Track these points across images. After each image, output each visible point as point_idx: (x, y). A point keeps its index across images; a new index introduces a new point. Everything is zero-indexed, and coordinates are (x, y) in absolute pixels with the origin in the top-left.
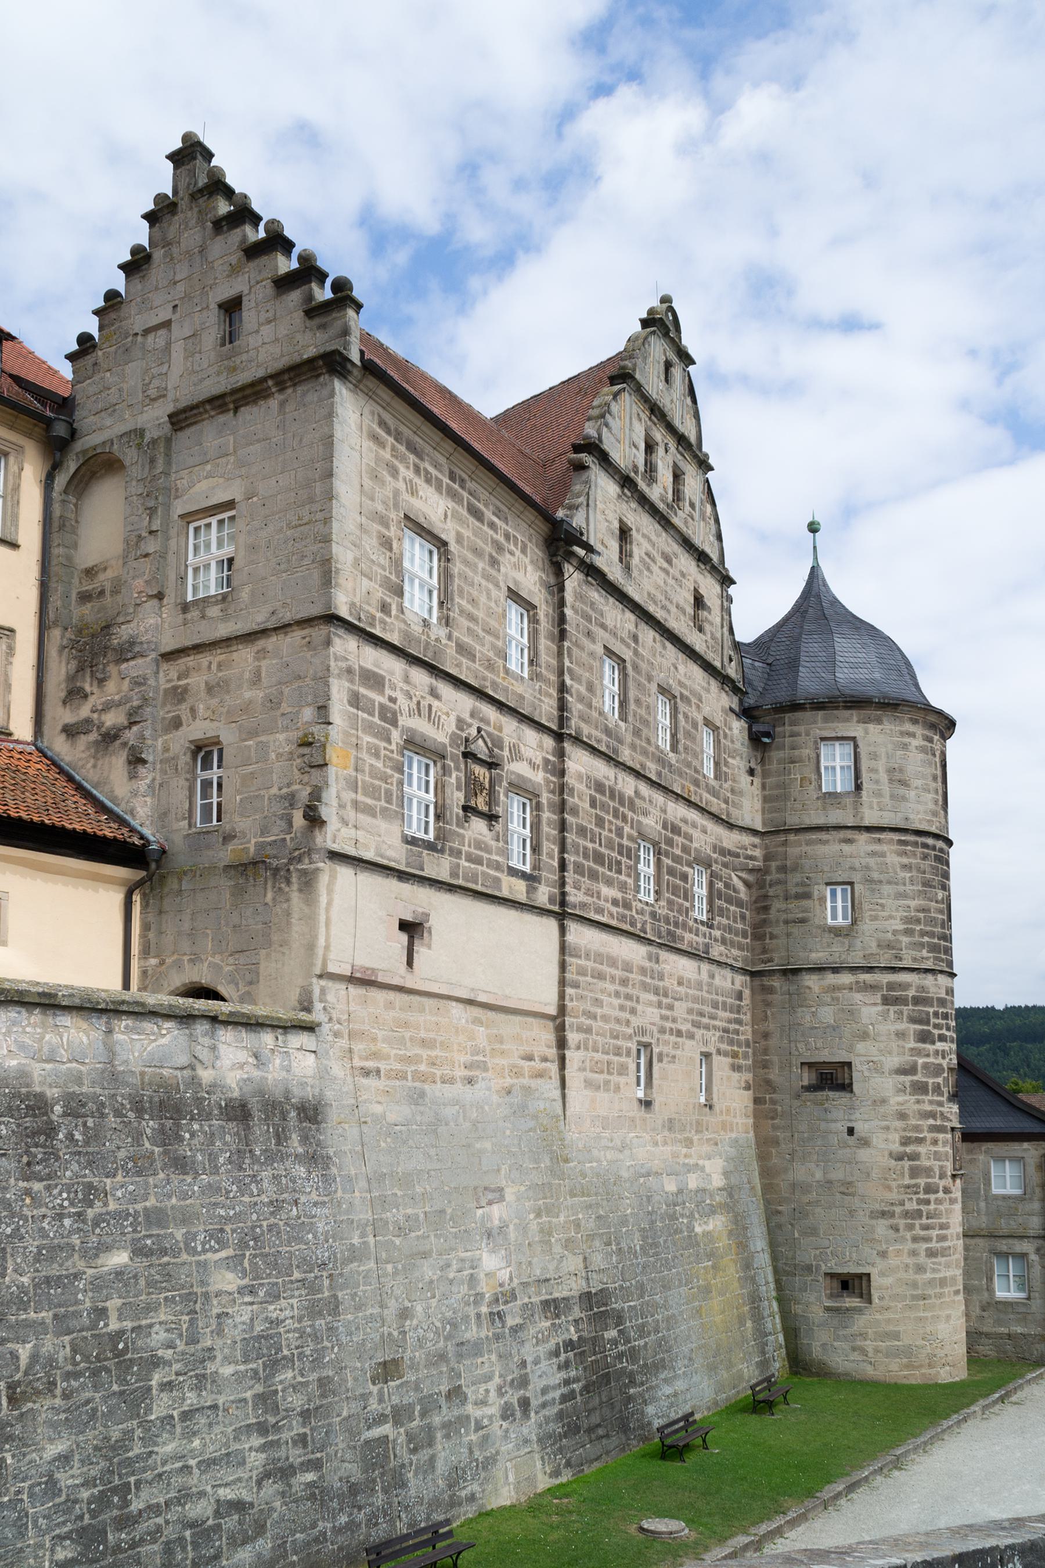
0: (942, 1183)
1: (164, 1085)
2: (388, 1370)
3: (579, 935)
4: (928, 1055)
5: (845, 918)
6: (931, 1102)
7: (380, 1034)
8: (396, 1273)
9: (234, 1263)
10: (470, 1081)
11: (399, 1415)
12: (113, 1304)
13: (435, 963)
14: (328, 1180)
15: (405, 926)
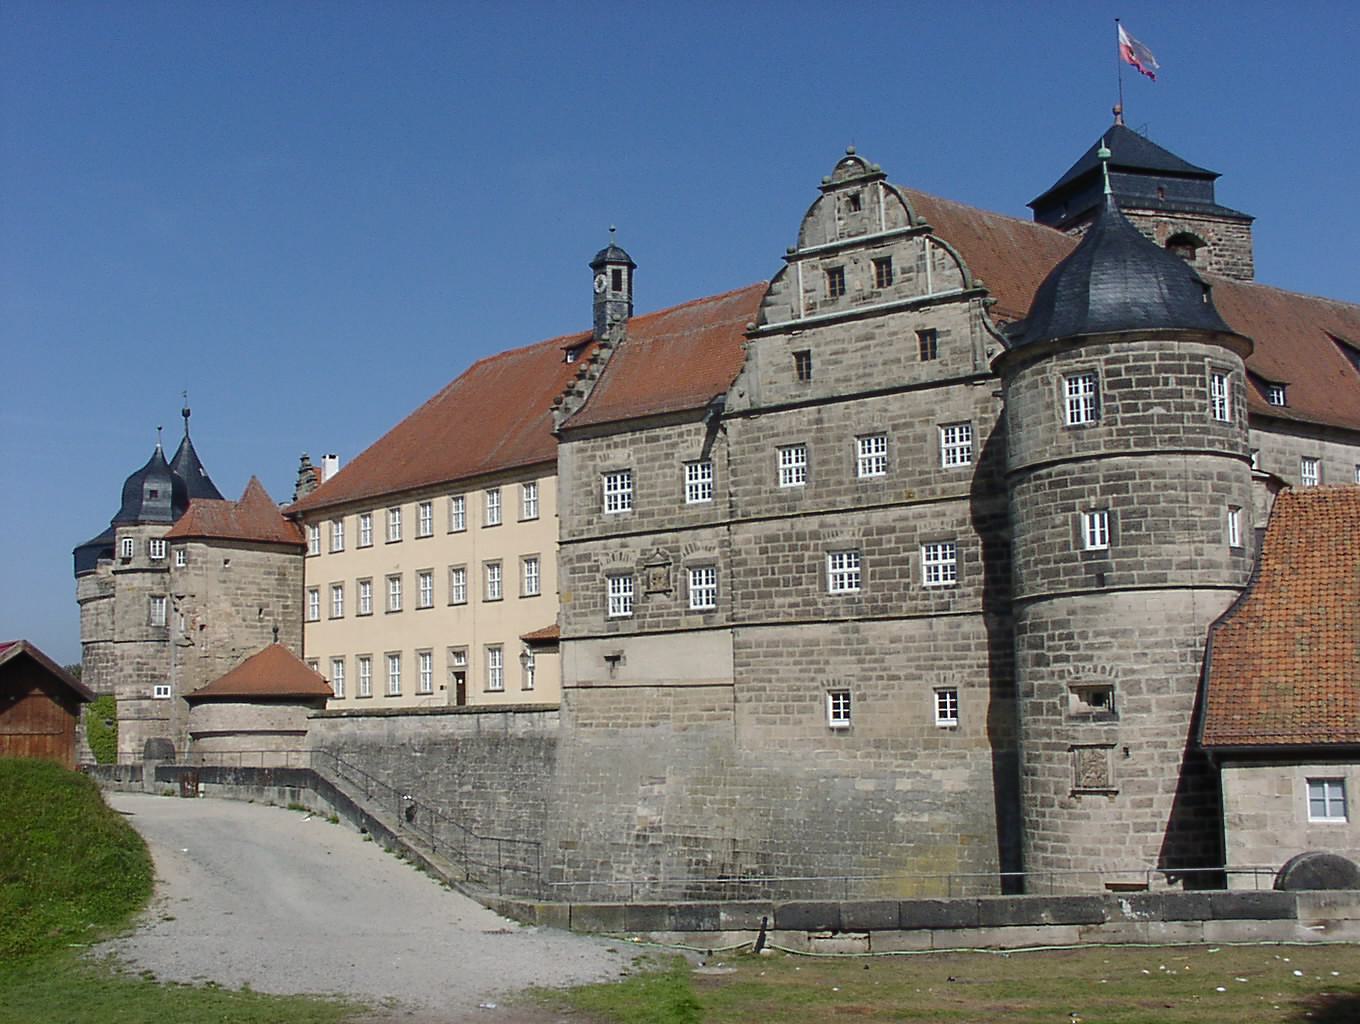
0: (1057, 799)
1: (495, 735)
2: (567, 845)
3: (744, 634)
4: (1042, 678)
5: (1103, 542)
6: (1046, 721)
7: (595, 708)
8: (578, 808)
9: (507, 794)
10: (653, 725)
11: (571, 863)
12: (464, 801)
13: (625, 673)
14: (552, 768)
15: (608, 659)
